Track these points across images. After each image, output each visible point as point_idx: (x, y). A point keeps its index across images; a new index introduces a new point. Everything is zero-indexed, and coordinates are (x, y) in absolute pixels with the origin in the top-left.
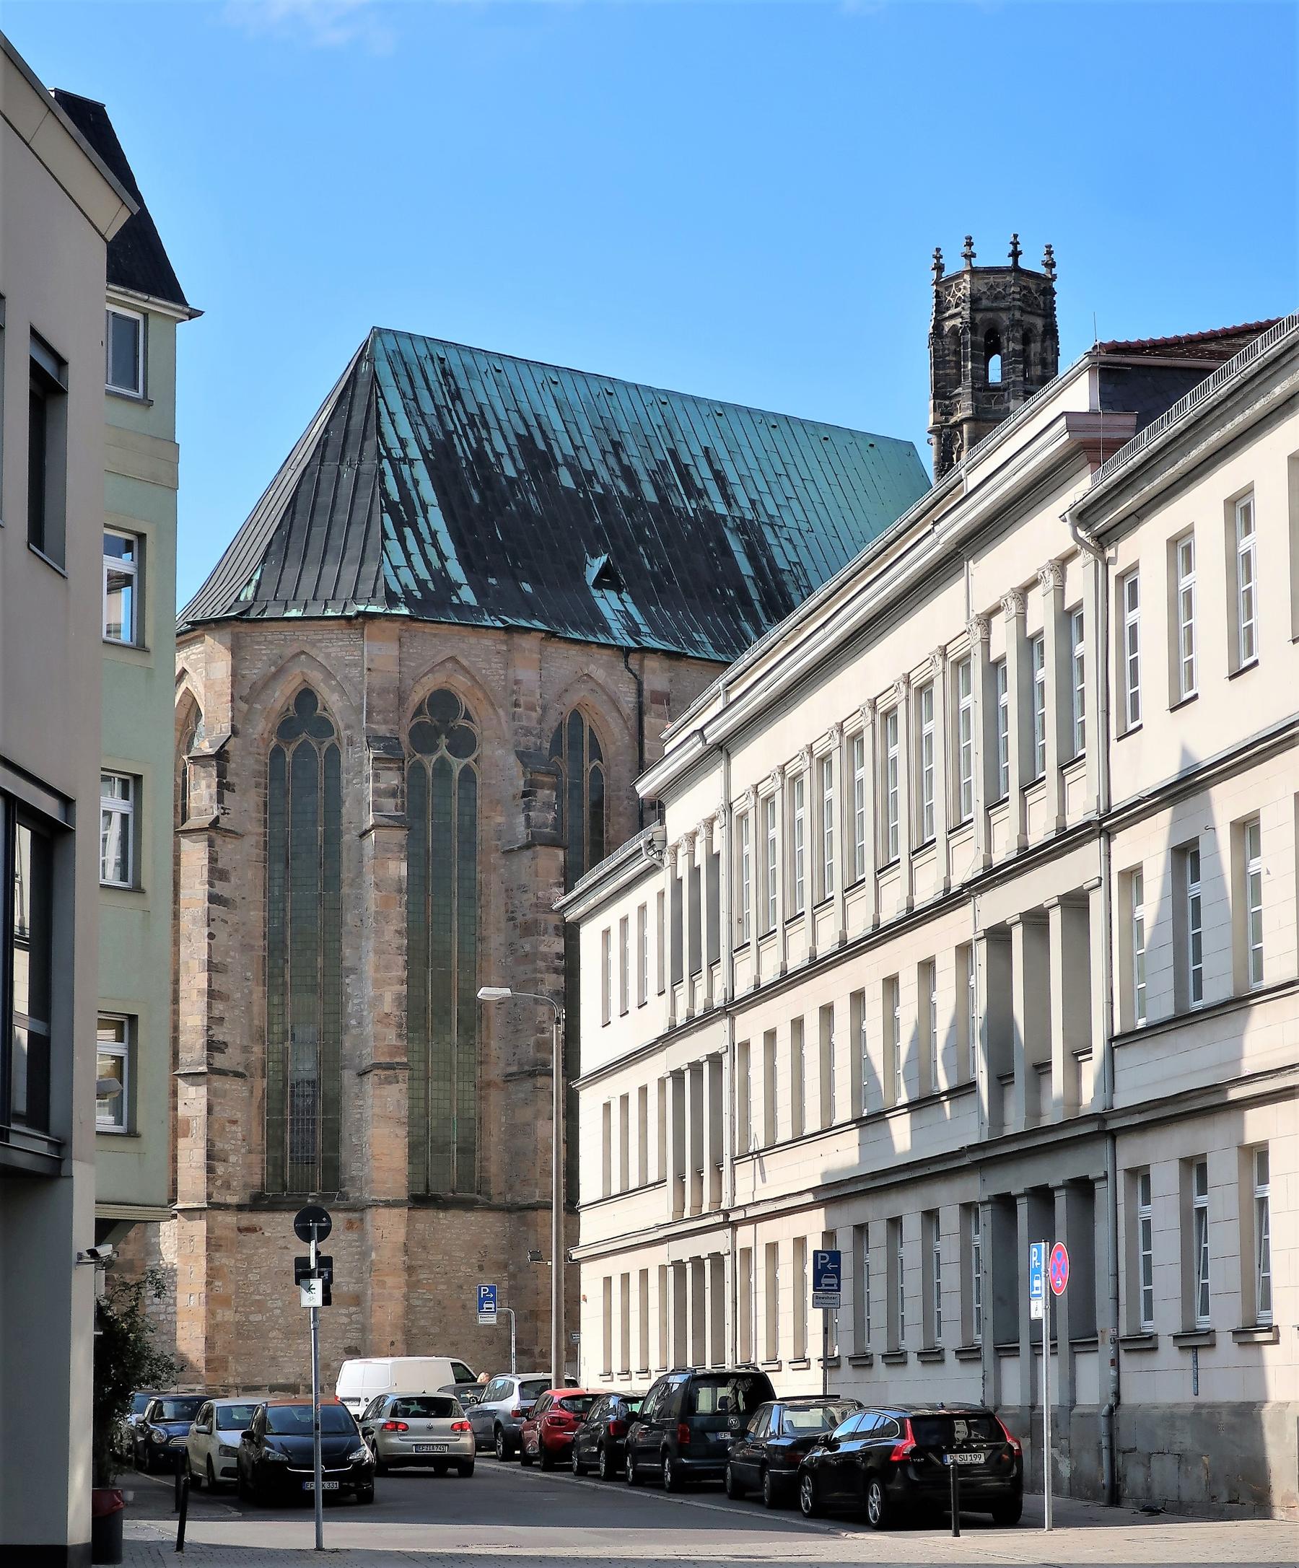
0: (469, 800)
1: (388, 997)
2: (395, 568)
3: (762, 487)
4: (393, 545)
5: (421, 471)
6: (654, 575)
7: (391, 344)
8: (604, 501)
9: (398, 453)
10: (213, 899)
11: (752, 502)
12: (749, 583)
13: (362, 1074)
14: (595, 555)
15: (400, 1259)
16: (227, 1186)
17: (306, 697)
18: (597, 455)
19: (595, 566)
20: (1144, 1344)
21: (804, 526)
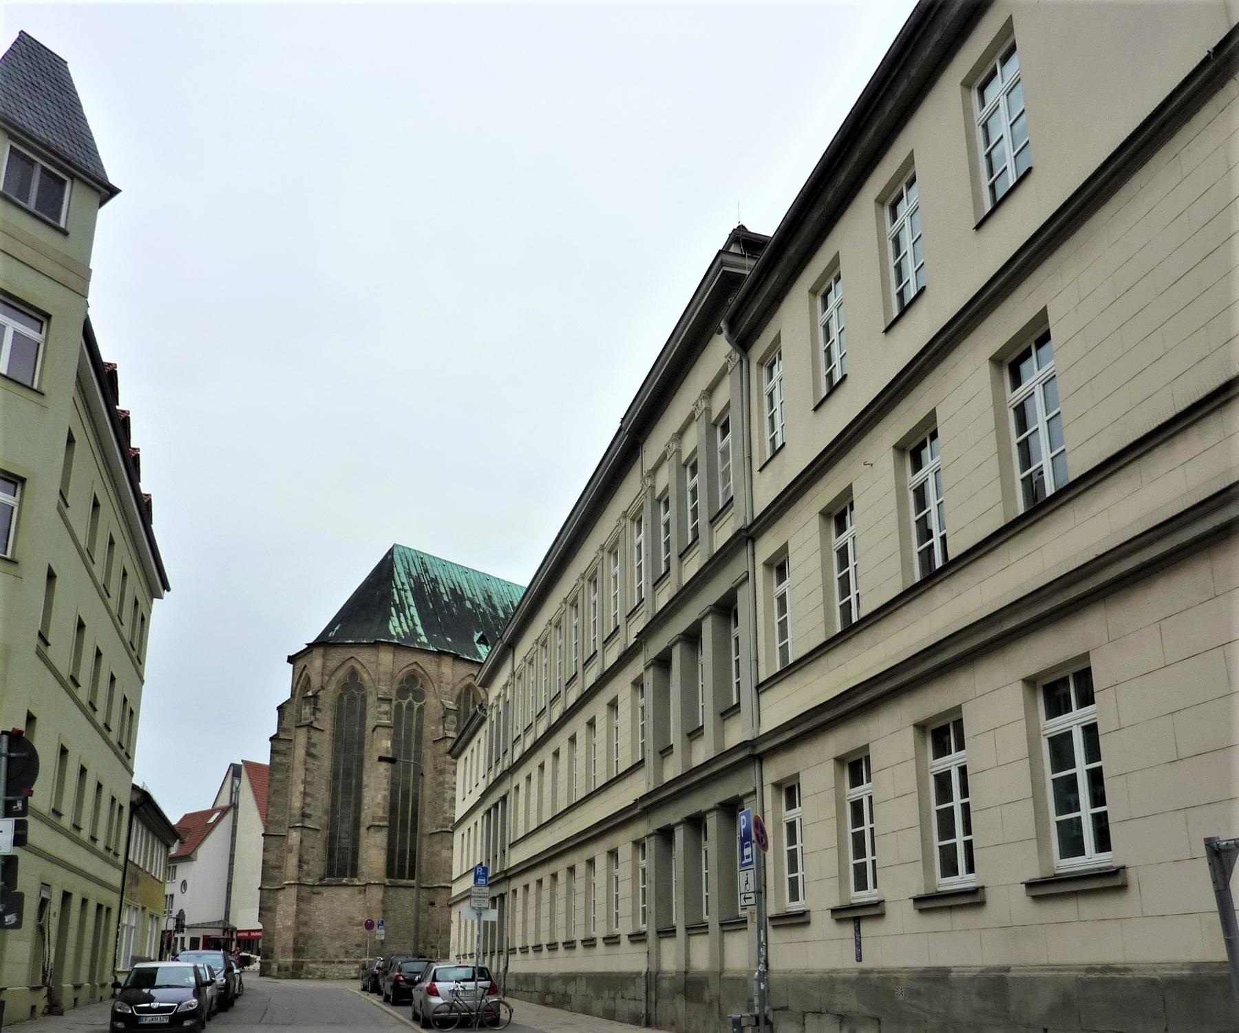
0: (420, 720)
1: (380, 796)
4: (395, 619)
5: (409, 594)
7: (401, 550)
8: (484, 614)
9: (400, 587)
10: (308, 754)
13: (368, 829)
15: (380, 906)
16: (308, 875)
17: (354, 674)
19: (477, 637)
20: (799, 920)
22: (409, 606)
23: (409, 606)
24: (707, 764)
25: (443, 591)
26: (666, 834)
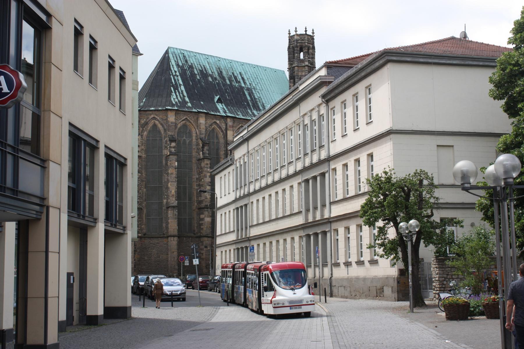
2: (174, 99)
3: (252, 80)
4: (174, 94)
7: (172, 50)
8: (218, 84)
9: (174, 74)
14: (217, 96)
18: (217, 74)
19: (216, 98)
20: (337, 265)
22: (180, 85)
23: (180, 85)
24: (318, 221)
25: (196, 72)
26: (308, 236)
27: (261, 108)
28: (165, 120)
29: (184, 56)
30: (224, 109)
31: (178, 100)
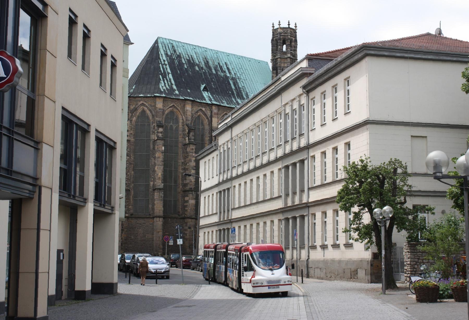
2: (162, 87)
3: (237, 71)
4: (162, 82)
5: (168, 67)
6: (214, 88)
7: (162, 40)
8: (205, 73)
9: (163, 63)
11: (235, 74)
12: (234, 90)
14: (203, 84)
18: (203, 63)
19: (203, 87)
20: (314, 247)
21: (245, 79)
22: (168, 73)
23: (168, 73)
24: (297, 205)
25: (184, 62)
26: (287, 219)
27: (245, 97)
28: (153, 106)
29: (172, 46)
30: (209, 97)
31: (166, 88)
